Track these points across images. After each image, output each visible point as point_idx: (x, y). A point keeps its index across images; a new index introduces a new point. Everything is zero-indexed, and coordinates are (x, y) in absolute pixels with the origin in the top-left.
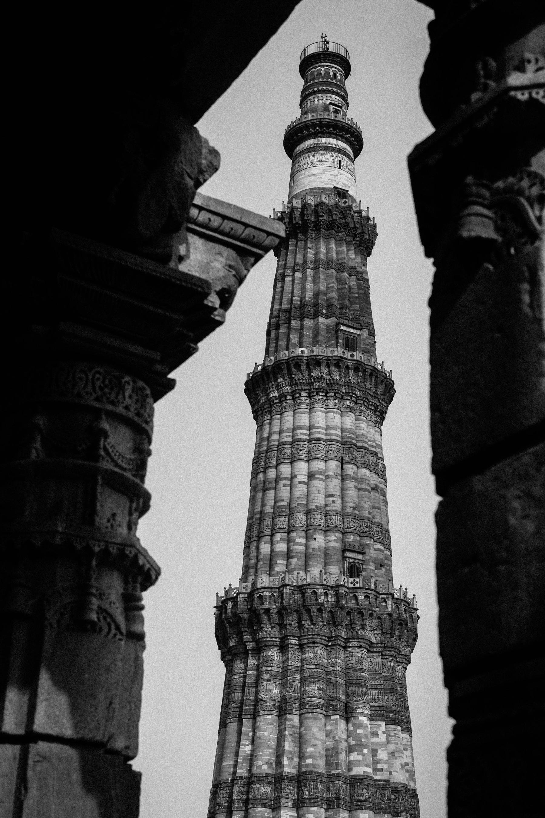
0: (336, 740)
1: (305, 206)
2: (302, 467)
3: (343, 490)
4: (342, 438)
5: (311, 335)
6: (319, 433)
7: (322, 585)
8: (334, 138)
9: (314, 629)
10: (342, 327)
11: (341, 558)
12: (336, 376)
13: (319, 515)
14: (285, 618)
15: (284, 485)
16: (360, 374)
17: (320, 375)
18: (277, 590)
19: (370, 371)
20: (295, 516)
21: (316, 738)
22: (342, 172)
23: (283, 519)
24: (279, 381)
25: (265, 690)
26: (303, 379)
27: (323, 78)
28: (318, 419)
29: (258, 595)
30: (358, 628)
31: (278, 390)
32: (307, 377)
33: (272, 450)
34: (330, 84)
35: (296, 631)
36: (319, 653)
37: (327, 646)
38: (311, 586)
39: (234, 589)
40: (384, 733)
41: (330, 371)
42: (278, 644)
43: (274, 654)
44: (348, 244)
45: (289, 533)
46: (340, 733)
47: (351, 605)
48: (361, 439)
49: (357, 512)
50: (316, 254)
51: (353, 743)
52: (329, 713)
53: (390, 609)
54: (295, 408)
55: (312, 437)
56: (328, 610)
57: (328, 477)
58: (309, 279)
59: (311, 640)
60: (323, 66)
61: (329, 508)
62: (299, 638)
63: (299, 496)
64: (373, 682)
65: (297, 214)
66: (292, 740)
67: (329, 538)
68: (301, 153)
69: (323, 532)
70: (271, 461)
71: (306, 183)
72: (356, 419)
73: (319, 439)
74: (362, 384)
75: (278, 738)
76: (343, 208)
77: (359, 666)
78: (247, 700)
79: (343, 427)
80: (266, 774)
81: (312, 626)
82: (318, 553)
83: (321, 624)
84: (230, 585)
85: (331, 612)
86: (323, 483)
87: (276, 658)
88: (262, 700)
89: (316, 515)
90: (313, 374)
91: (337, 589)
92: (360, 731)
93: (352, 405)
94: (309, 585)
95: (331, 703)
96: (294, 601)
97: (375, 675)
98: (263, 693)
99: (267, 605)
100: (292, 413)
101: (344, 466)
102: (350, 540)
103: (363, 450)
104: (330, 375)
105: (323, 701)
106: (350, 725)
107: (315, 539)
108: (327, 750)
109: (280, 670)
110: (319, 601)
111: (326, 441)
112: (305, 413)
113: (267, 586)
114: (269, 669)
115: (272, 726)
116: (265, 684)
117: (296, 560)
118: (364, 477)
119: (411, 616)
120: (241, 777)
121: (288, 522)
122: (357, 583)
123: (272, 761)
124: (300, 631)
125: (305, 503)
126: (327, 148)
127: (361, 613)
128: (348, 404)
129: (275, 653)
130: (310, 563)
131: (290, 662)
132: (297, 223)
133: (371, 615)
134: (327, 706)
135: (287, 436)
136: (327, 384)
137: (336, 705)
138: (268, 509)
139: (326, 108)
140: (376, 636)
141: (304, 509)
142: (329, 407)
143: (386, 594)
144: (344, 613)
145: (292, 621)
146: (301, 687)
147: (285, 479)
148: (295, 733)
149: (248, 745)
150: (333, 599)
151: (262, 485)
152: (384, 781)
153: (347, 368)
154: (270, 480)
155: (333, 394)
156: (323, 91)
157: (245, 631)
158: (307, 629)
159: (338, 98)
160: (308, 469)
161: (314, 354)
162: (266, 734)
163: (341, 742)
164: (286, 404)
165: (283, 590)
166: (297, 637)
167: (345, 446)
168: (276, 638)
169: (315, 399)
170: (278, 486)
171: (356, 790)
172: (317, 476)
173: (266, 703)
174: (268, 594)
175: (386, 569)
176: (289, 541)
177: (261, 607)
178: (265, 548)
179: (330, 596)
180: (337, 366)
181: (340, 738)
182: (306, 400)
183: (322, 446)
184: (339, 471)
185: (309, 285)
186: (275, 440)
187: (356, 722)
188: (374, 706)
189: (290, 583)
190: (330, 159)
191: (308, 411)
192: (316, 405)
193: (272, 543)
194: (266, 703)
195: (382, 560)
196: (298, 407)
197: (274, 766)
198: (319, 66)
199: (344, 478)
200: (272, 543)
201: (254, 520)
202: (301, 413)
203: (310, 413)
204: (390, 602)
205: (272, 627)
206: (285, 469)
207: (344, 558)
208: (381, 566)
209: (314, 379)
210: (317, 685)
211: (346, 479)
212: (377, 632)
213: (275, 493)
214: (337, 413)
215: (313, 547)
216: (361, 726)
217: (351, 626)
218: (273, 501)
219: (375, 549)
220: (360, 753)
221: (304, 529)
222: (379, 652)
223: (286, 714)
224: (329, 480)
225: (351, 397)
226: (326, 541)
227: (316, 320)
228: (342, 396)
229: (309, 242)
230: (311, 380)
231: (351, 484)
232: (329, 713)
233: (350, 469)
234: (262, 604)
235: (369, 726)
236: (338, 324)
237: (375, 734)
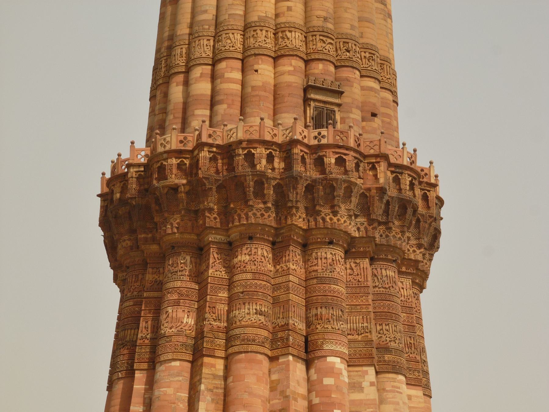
11: (301, 101)
13: (264, 32)
20: (224, 36)
21: (251, 394)
23: (206, 42)
29: (159, 165)
36: (259, 253)
39: (125, 161)
40: (372, 384)
45: (213, 65)
46: (292, 384)
49: (330, 26)
56: (274, 183)
61: (281, 20)
64: (355, 302)
66: (213, 400)
67: (280, 69)
69: (271, 60)
77: (328, 274)
82: (262, 93)
83: (262, 206)
84: (119, 155)
89: (259, 31)
92: (328, 381)
94: (240, 142)
95: (280, 335)
97: (358, 291)
102: (316, 71)
105: (265, 333)
106: (312, 371)
107: (256, 71)
110: (258, 167)
114: (179, 284)
115: (181, 378)
116: (170, 310)
117: (225, 106)
119: (425, 198)
121: (214, 46)
122: (323, 137)
125: (242, 13)
129: (188, 258)
130: (248, 110)
131: (211, 271)
137: (288, 339)
138: (183, 30)
140: (359, 225)
141: (240, 24)
146: (229, 312)
148: (217, 388)
150: (282, 165)
162: (170, 391)
163: (296, 400)
173: (170, 341)
175: (383, 121)
176: (213, 77)
178: (176, 92)
179: (276, 160)
181: (294, 393)
188: (355, 341)
189: (210, 141)
193: (186, 83)
195: (374, 104)
200: (186, 83)
204: (382, 168)
207: (306, 101)
208: (374, 115)
210: (253, 308)
212: (361, 220)
215: (254, 83)
216: (332, 371)
219: (363, 88)
221: (240, 56)
226: (277, 75)
235: (345, 373)
237: (355, 386)
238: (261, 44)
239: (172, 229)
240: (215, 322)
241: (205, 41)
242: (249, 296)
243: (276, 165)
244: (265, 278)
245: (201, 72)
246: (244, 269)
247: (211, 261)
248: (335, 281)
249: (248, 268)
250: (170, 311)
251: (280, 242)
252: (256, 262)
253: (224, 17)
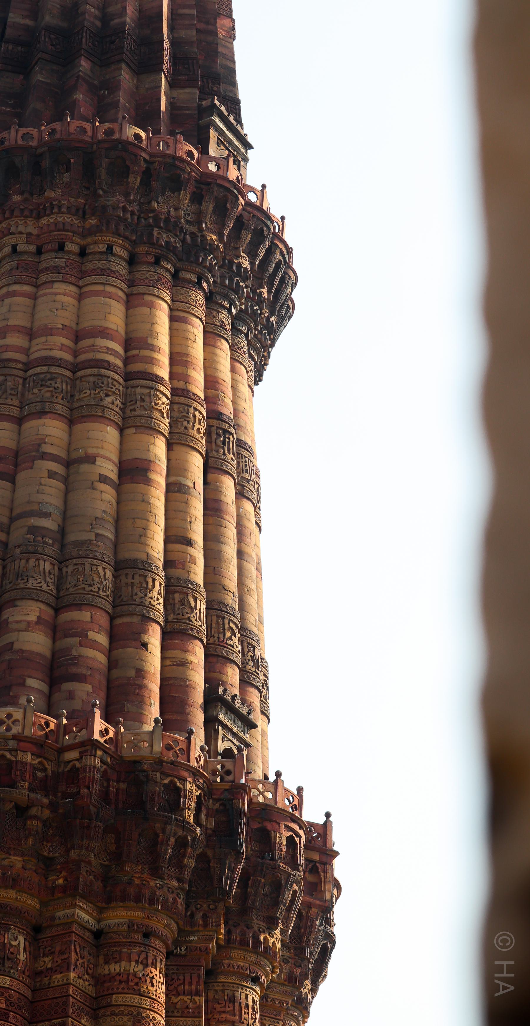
15: (52, 475)
87: (22, 957)
94: (160, 762)
99: (22, 792)
129: (21, 939)
167: (214, 422)
174: (28, 758)
238: (153, 603)
241: (48, 564)
243: (203, 820)
245: (38, 614)
246: (136, 988)
251: (180, 955)
252: (154, 981)
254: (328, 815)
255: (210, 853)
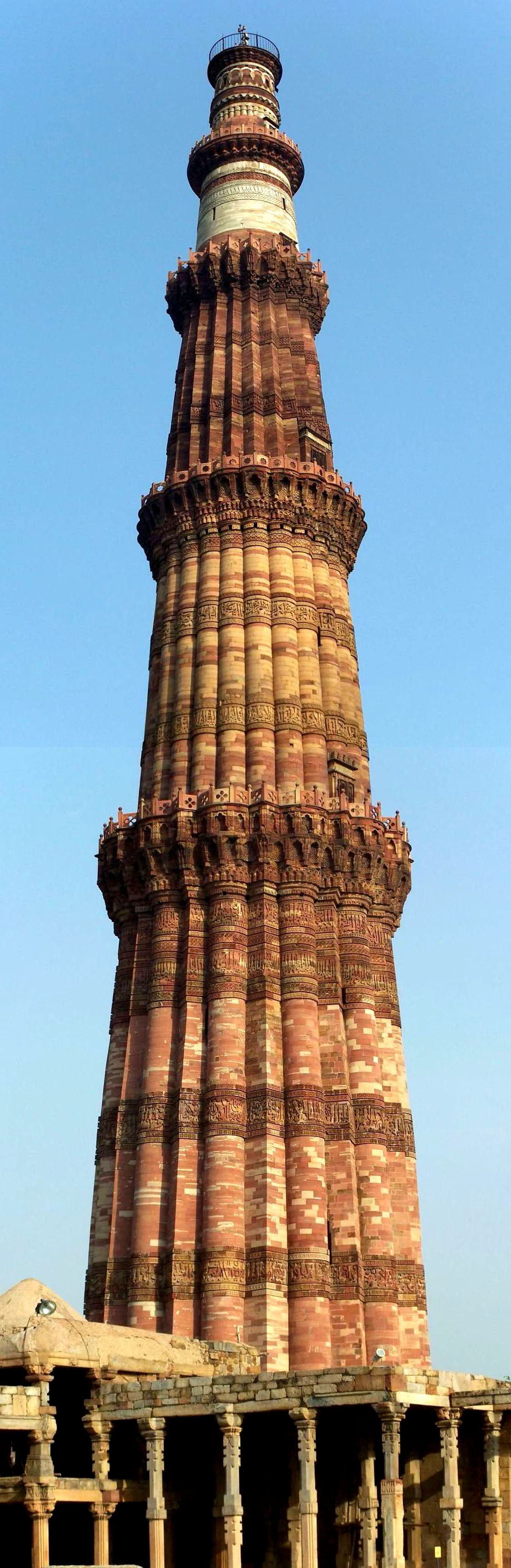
0: (339, 1042)
1: (247, 252)
2: (263, 635)
3: (322, 676)
4: (316, 598)
5: (263, 439)
6: (288, 586)
7: (318, 809)
8: (274, 165)
9: (305, 873)
10: (310, 435)
12: (310, 504)
14: (261, 853)
16: (340, 507)
17: (287, 499)
18: (246, 810)
19: (351, 506)
22: (287, 215)
24: (221, 499)
25: (227, 961)
26: (261, 502)
27: (254, 82)
28: (285, 566)
29: (217, 814)
30: (361, 878)
31: (217, 513)
32: (267, 499)
33: (209, 603)
34: (263, 92)
35: (274, 875)
37: (316, 901)
38: (304, 809)
41: (301, 496)
42: (244, 892)
43: (238, 906)
44: (303, 317)
47: (353, 843)
48: (338, 604)
49: (342, 711)
50: (262, 323)
51: (357, 1047)
52: (323, 1001)
53: (400, 856)
54: (248, 544)
55: (277, 590)
57: (302, 654)
58: (256, 357)
59: (299, 890)
60: (253, 67)
62: (279, 887)
63: (262, 677)
65: (235, 260)
68: (225, 178)
70: (207, 620)
71: (239, 220)
72: (331, 574)
73: (288, 595)
74: (338, 523)
75: (247, 1033)
76: (302, 264)
78: (191, 973)
79: (318, 582)
80: (237, 1086)
81: (302, 869)
83: (314, 867)
85: (328, 850)
86: (296, 661)
87: (240, 915)
88: (223, 975)
90: (276, 497)
91: (338, 816)
93: (326, 552)
94: (300, 806)
96: (275, 828)
98: (224, 965)
99: (232, 832)
100: (241, 551)
101: (322, 641)
103: (342, 621)
104: (302, 501)
108: (323, 1055)
109: (246, 932)
110: (315, 832)
111: (299, 599)
112: (263, 553)
113: (232, 801)
115: (240, 1016)
116: (226, 951)
118: (346, 661)
120: (189, 1090)
123: (241, 1068)
124: (281, 875)
126: (267, 178)
127: (368, 857)
128: (322, 549)
129: (239, 905)
132: (233, 274)
133: (379, 861)
134: (320, 992)
135: (236, 586)
136: (296, 514)
138: (209, 691)
139: (261, 122)
142: (298, 549)
143: (395, 833)
144: (346, 853)
145: (270, 857)
146: (282, 960)
147: (237, 649)
149: (196, 1042)
151: (191, 655)
152: (394, 1104)
153: (325, 494)
154: (210, 649)
155: (303, 532)
156: (255, 100)
157: (188, 869)
158: (295, 873)
159: (273, 114)
160: (273, 639)
161: (281, 466)
162: (233, 1026)
164: (231, 537)
165: (259, 811)
166: (277, 884)
167: (321, 610)
168: (242, 882)
169: (278, 534)
170: (224, 659)
171: (366, 1115)
172: (288, 650)
173: (230, 981)
174: (233, 814)
177: (221, 833)
178: (207, 749)
180: (313, 489)
182: (263, 534)
183: (293, 606)
184: (316, 647)
185: (256, 366)
186: (214, 589)
187: (359, 1016)
190: (272, 193)
191: (267, 550)
192: (281, 545)
194: (230, 981)
196: (253, 543)
197: (244, 1075)
198: (247, 66)
199: (323, 659)
201: (180, 707)
202: (258, 552)
203: (270, 554)
205: (238, 865)
206: (236, 634)
209: (279, 503)
211: (326, 660)
213: (219, 669)
214: (309, 560)
217: (353, 874)
218: (216, 682)
220: (369, 1063)
222: (380, 917)
223: (264, 998)
224: (306, 658)
225: (326, 539)
227: (268, 418)
228: (314, 537)
229: (252, 304)
230: (273, 505)
231: (333, 669)
232: (323, 1001)
233: (330, 645)
234: (225, 829)
236: (303, 430)
239: (228, 876)
240: (270, 970)
242: (301, 948)
243: (326, 831)
244: (313, 932)
247: (265, 910)
248: (364, 941)
249: (302, 922)
250: (227, 953)
253: (255, 689)
254: (397, 813)
255: (331, 848)
